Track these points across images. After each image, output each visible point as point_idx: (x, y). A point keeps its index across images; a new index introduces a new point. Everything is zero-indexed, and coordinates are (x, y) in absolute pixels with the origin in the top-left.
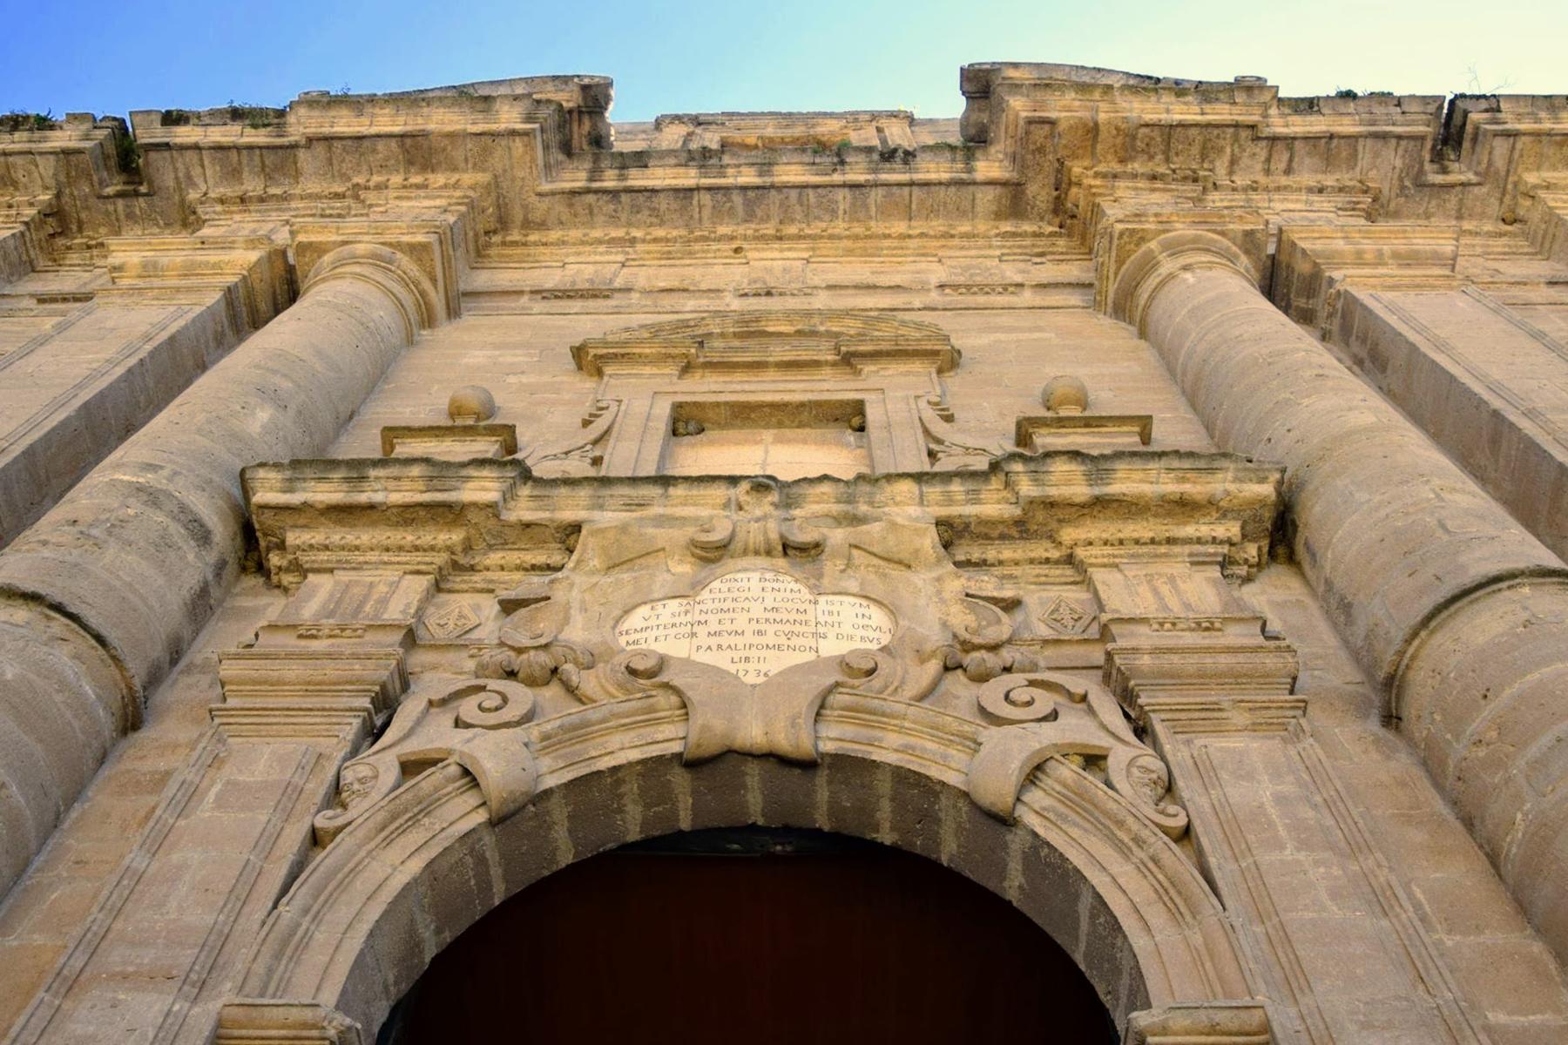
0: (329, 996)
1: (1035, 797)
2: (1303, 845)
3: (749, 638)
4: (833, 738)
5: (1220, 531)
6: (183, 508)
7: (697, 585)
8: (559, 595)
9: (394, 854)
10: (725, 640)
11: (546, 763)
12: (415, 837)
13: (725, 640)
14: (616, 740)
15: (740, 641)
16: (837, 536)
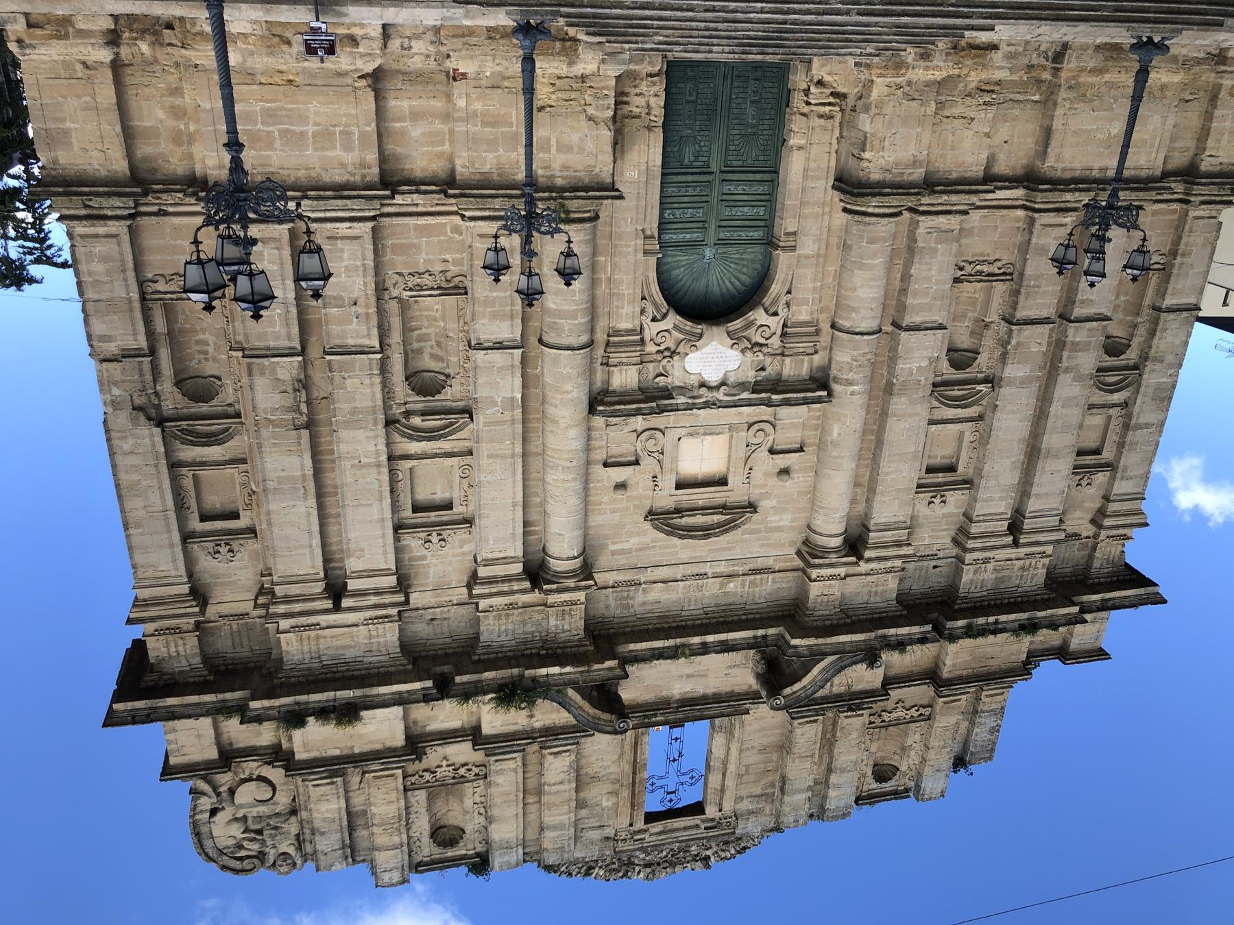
0: (781, 258)
1: (664, 311)
2: (624, 294)
3: (714, 356)
4: (699, 328)
5: (609, 399)
6: (841, 384)
7: (725, 374)
8: (754, 373)
9: (776, 291)
10: (719, 355)
11: (752, 318)
12: (773, 296)
13: (719, 355)
14: (739, 326)
15: (717, 355)
16: (695, 394)
